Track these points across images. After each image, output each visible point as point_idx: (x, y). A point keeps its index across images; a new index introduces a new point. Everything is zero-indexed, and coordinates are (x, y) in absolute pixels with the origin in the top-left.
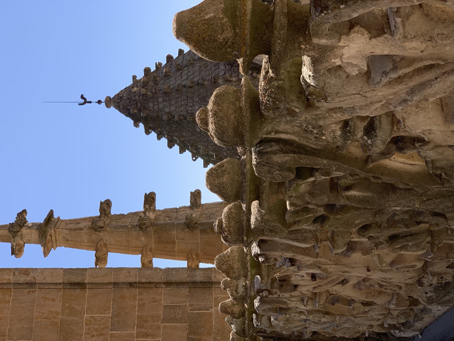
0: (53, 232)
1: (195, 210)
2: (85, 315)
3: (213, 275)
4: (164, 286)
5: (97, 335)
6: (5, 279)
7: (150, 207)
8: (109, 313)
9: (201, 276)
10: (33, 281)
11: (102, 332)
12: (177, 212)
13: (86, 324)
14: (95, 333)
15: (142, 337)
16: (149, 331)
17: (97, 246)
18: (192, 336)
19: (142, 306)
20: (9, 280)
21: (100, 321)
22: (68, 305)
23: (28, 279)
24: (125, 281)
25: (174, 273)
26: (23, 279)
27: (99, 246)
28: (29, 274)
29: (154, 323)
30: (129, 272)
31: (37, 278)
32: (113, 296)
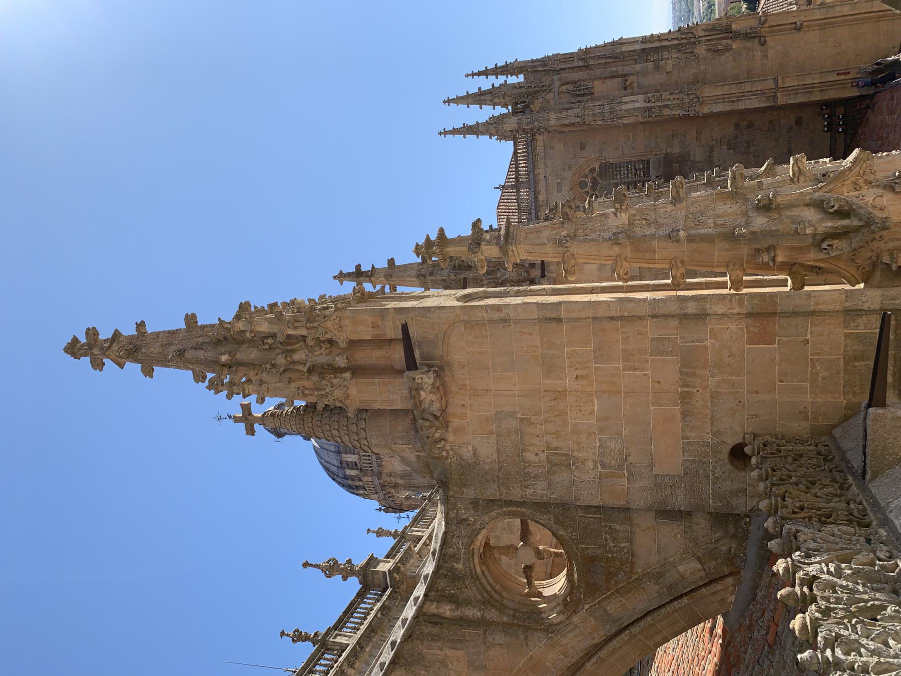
0: (514, 249)
1: (678, 206)
3: (708, 306)
4: (650, 318)
5: (581, 369)
6: (479, 317)
7: (621, 206)
9: (694, 307)
10: (507, 317)
11: (586, 365)
12: (654, 209)
13: (568, 358)
14: (578, 366)
18: (685, 370)
20: (482, 317)
21: (582, 354)
22: (546, 339)
23: (502, 315)
24: (605, 316)
25: (661, 305)
26: (497, 315)
27: (566, 258)
28: (502, 310)
30: (609, 306)
31: (511, 314)
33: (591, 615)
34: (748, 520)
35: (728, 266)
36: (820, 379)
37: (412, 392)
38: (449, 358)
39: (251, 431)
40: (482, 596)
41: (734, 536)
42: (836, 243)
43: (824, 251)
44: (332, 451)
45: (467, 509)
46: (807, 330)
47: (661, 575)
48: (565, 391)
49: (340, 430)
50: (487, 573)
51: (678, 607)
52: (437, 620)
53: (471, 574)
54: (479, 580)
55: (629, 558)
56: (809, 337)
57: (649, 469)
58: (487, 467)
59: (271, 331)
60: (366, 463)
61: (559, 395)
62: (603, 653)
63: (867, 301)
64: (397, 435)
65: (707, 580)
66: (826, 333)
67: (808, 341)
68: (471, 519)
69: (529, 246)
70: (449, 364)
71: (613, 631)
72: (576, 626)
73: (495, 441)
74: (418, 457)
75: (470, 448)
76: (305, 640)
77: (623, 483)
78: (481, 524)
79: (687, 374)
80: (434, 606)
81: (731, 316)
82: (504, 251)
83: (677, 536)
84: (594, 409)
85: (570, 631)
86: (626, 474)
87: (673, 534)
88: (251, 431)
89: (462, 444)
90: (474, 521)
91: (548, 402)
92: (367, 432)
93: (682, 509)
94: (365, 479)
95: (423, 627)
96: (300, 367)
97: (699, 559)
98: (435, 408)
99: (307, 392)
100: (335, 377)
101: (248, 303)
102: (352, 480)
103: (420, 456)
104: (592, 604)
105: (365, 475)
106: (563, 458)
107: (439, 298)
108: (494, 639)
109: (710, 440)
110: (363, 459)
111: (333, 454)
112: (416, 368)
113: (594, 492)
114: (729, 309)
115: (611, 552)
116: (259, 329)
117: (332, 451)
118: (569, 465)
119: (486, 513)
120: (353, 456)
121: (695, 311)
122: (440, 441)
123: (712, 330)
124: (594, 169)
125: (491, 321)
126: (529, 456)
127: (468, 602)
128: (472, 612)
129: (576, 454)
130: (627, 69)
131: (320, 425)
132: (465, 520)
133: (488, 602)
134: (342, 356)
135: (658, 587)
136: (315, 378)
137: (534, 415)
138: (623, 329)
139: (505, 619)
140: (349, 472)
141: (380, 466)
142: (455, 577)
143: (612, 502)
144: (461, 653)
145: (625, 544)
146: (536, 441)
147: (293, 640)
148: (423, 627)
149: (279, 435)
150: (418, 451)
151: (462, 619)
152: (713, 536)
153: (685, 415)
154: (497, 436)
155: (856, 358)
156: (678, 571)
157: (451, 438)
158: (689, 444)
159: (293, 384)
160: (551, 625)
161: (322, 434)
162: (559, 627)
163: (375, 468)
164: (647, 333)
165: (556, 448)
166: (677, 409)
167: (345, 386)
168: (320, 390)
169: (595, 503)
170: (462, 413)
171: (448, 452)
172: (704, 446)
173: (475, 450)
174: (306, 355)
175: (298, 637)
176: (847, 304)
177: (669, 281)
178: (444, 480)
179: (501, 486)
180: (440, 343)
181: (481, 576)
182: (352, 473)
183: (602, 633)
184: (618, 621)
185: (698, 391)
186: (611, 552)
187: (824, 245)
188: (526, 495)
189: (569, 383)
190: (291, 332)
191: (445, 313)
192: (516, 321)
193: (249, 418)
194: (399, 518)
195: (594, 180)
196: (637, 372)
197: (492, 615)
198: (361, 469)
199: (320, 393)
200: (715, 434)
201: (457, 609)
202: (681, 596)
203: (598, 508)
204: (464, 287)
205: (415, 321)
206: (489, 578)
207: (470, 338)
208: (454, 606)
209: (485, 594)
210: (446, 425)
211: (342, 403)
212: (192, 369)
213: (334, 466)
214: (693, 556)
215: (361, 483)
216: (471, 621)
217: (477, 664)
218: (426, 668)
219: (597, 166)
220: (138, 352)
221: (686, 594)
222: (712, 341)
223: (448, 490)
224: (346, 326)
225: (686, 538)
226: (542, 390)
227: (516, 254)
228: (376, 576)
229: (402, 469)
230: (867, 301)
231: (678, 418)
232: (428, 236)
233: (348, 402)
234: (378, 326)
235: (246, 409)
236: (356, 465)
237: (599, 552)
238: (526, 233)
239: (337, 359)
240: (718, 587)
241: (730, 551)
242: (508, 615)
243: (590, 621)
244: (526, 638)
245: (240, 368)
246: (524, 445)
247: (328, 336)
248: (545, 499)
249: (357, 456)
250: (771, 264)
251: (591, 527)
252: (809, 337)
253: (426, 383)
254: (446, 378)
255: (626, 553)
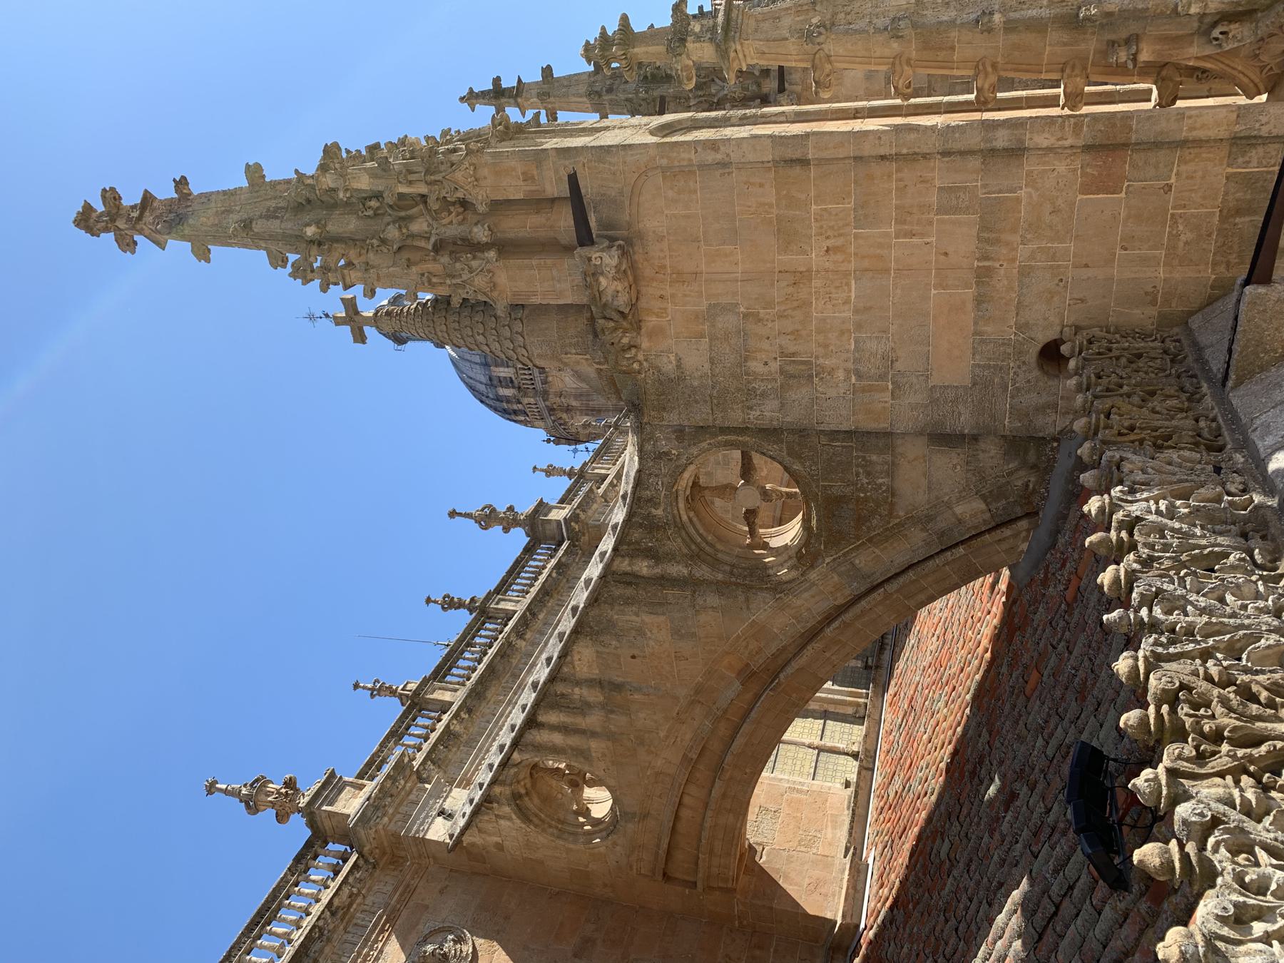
0: (739, 47)
2: (814, 207)
4: (939, 156)
5: (835, 236)
6: (683, 160)
8: (849, 203)
9: (1006, 138)
10: (727, 159)
11: (841, 231)
13: (816, 220)
15: (905, 236)
16: (915, 228)
17: (813, 61)
18: (985, 235)
19: (902, 190)
20: (690, 160)
21: (837, 214)
22: (785, 192)
23: (719, 157)
24: (874, 153)
25: (957, 135)
26: (711, 157)
27: (817, 61)
28: (719, 149)
29: (923, 216)
30: (880, 138)
31: (732, 154)
32: (855, 176)
33: (833, 570)
34: (1055, 444)
35: (1063, 71)
36: (1181, 244)
37: (588, 279)
38: (641, 226)
39: (360, 337)
40: (690, 549)
41: (1034, 467)
42: (1234, 28)
43: (1215, 43)
44: (476, 363)
45: (667, 439)
46: (1171, 170)
47: (930, 518)
48: (809, 271)
49: (487, 334)
50: (695, 519)
51: (950, 558)
52: (631, 579)
53: (675, 522)
54: (684, 529)
55: (887, 497)
56: (1173, 181)
57: (923, 378)
58: (696, 383)
59: (374, 188)
60: (527, 379)
61: (801, 277)
62: (847, 617)
63: (1267, 123)
64: (567, 341)
65: (993, 524)
66: (1200, 173)
67: (1171, 186)
68: (673, 452)
69: (761, 43)
70: (641, 236)
71: (863, 589)
72: (814, 584)
73: (707, 346)
74: (599, 371)
75: (672, 358)
76: (458, 608)
77: (885, 399)
78: (688, 459)
79: (987, 241)
80: (626, 562)
81: (1060, 151)
82: (723, 52)
83: (956, 468)
84: (850, 296)
85: (806, 590)
86: (890, 387)
87: (951, 465)
88: (360, 337)
89: (661, 352)
90: (678, 455)
91: (784, 288)
92: (526, 337)
93: (966, 431)
94: (525, 401)
95: (613, 589)
96: (422, 244)
97: (984, 498)
98: (622, 301)
99: (434, 280)
100: (474, 258)
101: (336, 145)
102: (508, 402)
103: (601, 370)
104: (835, 556)
105: (525, 395)
106: (803, 367)
107: (623, 130)
108: (705, 601)
109: (1012, 337)
110: (521, 374)
111: (478, 367)
112: (592, 243)
113: (844, 412)
114: (1058, 140)
115: (865, 491)
116: (356, 185)
117: (476, 363)
118: (811, 376)
119: (694, 444)
120: (506, 370)
121: (1006, 144)
122: (629, 348)
123: (1029, 173)
125: (703, 167)
126: (755, 366)
127: (670, 557)
128: (676, 569)
129: (821, 361)
131: (457, 328)
132: (666, 454)
133: (696, 556)
134: (483, 226)
135: (925, 534)
136: (445, 259)
137: (764, 308)
138: (899, 175)
139: (720, 576)
140: (504, 392)
141: (545, 382)
142: (652, 526)
143: (872, 426)
144: (662, 618)
145: (883, 480)
146: (765, 345)
147: (443, 608)
148: (613, 589)
149: (399, 340)
150: (599, 363)
151: (662, 577)
152: (1006, 467)
153: (979, 301)
154: (711, 340)
155: (1238, 212)
156: (954, 514)
157: (645, 344)
158: (983, 341)
159: (414, 269)
160: (781, 583)
161: (462, 341)
162: (789, 586)
163: (539, 386)
164: (933, 179)
165: (793, 354)
166: (970, 292)
167: (489, 271)
168: (454, 277)
169: (844, 427)
170: (661, 309)
171: (641, 364)
172: (1004, 344)
173: (679, 360)
174: (429, 225)
175: (450, 604)
176: (1237, 128)
177: (972, 97)
178: (637, 402)
179: (715, 408)
180: (627, 203)
181: (688, 524)
182: (508, 392)
183: (847, 592)
184: (869, 577)
185: (1001, 265)
186: (863, 489)
187: (1216, 33)
188: (749, 418)
189: (815, 258)
190: (403, 189)
191: (632, 155)
192: (740, 166)
193: (356, 318)
194: (575, 451)
196: (915, 240)
197: (703, 572)
198: (519, 388)
199: (454, 281)
200: (1021, 327)
201: (657, 564)
202: (957, 545)
203: (849, 434)
204: (661, 113)
205: (588, 168)
206: (699, 526)
207: (670, 194)
208: (652, 562)
209: (693, 547)
210: (638, 326)
211: (487, 296)
212: (265, 249)
213: (481, 383)
214: (977, 494)
215: (520, 406)
216: (675, 580)
217: (683, 632)
218: (618, 637)
220: (183, 225)
221: (962, 542)
222: (1029, 190)
223: (643, 414)
224: (485, 178)
225: (968, 471)
226: (777, 270)
227: (741, 56)
228: (548, 527)
229: (575, 386)
230: (1267, 123)
231: (970, 306)
232: (603, 28)
233: (495, 294)
234: (533, 178)
235: (350, 305)
236: (512, 381)
237: (848, 491)
238: (757, 21)
239: (475, 230)
240: (1007, 532)
241: (1027, 486)
242: (724, 572)
243: (833, 577)
244: (747, 599)
245: (335, 245)
246: (749, 351)
247: (460, 195)
248: (775, 423)
249: (512, 370)
250: (1130, 66)
251: (838, 459)
252: (1173, 181)
253: (607, 265)
254: (636, 257)
255: (884, 492)
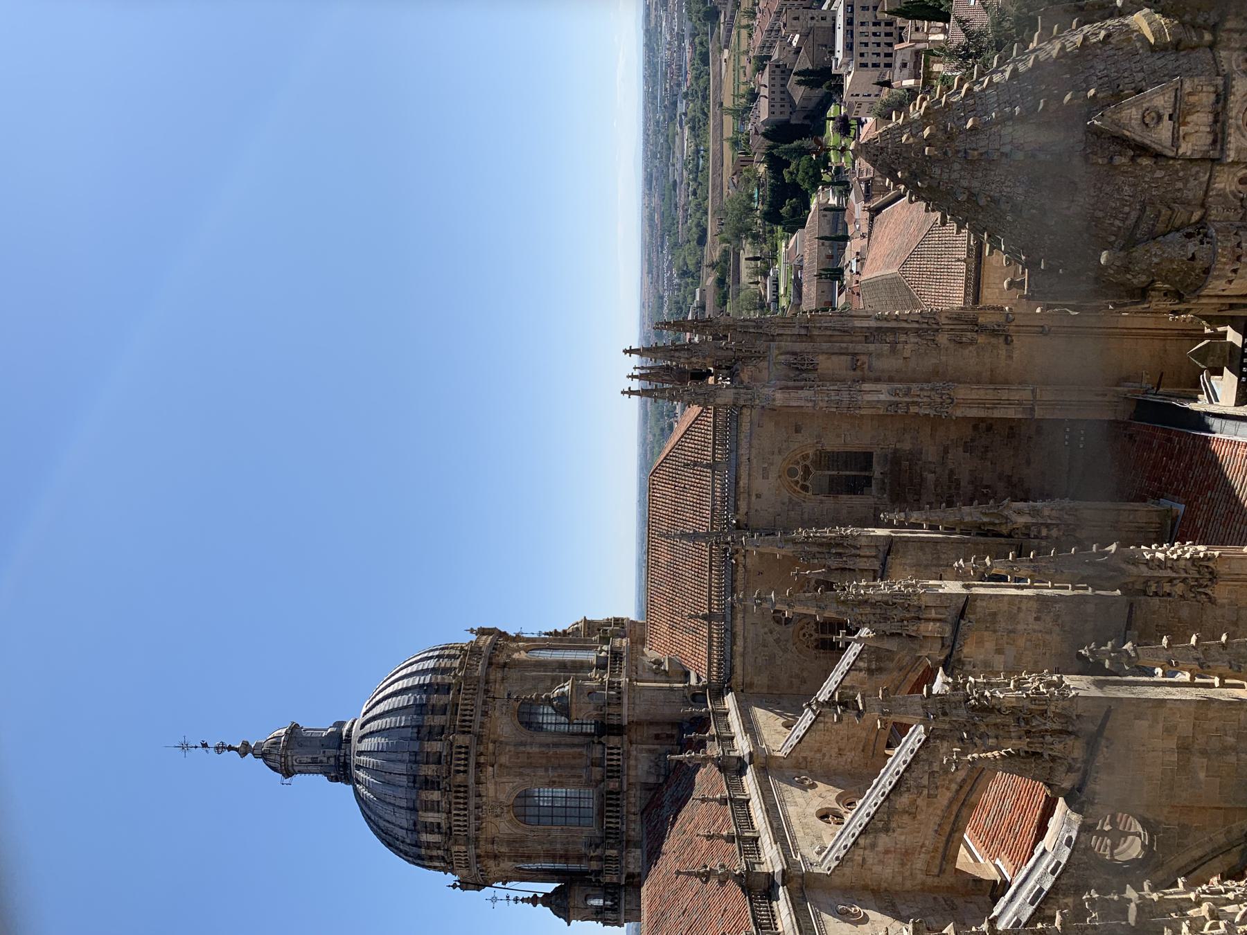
111: (403, 811)
120: (436, 815)
124: (807, 455)
130: (860, 348)
140: (425, 837)
194: (494, 900)
195: (806, 470)
219: (811, 452)
229: (510, 832)
